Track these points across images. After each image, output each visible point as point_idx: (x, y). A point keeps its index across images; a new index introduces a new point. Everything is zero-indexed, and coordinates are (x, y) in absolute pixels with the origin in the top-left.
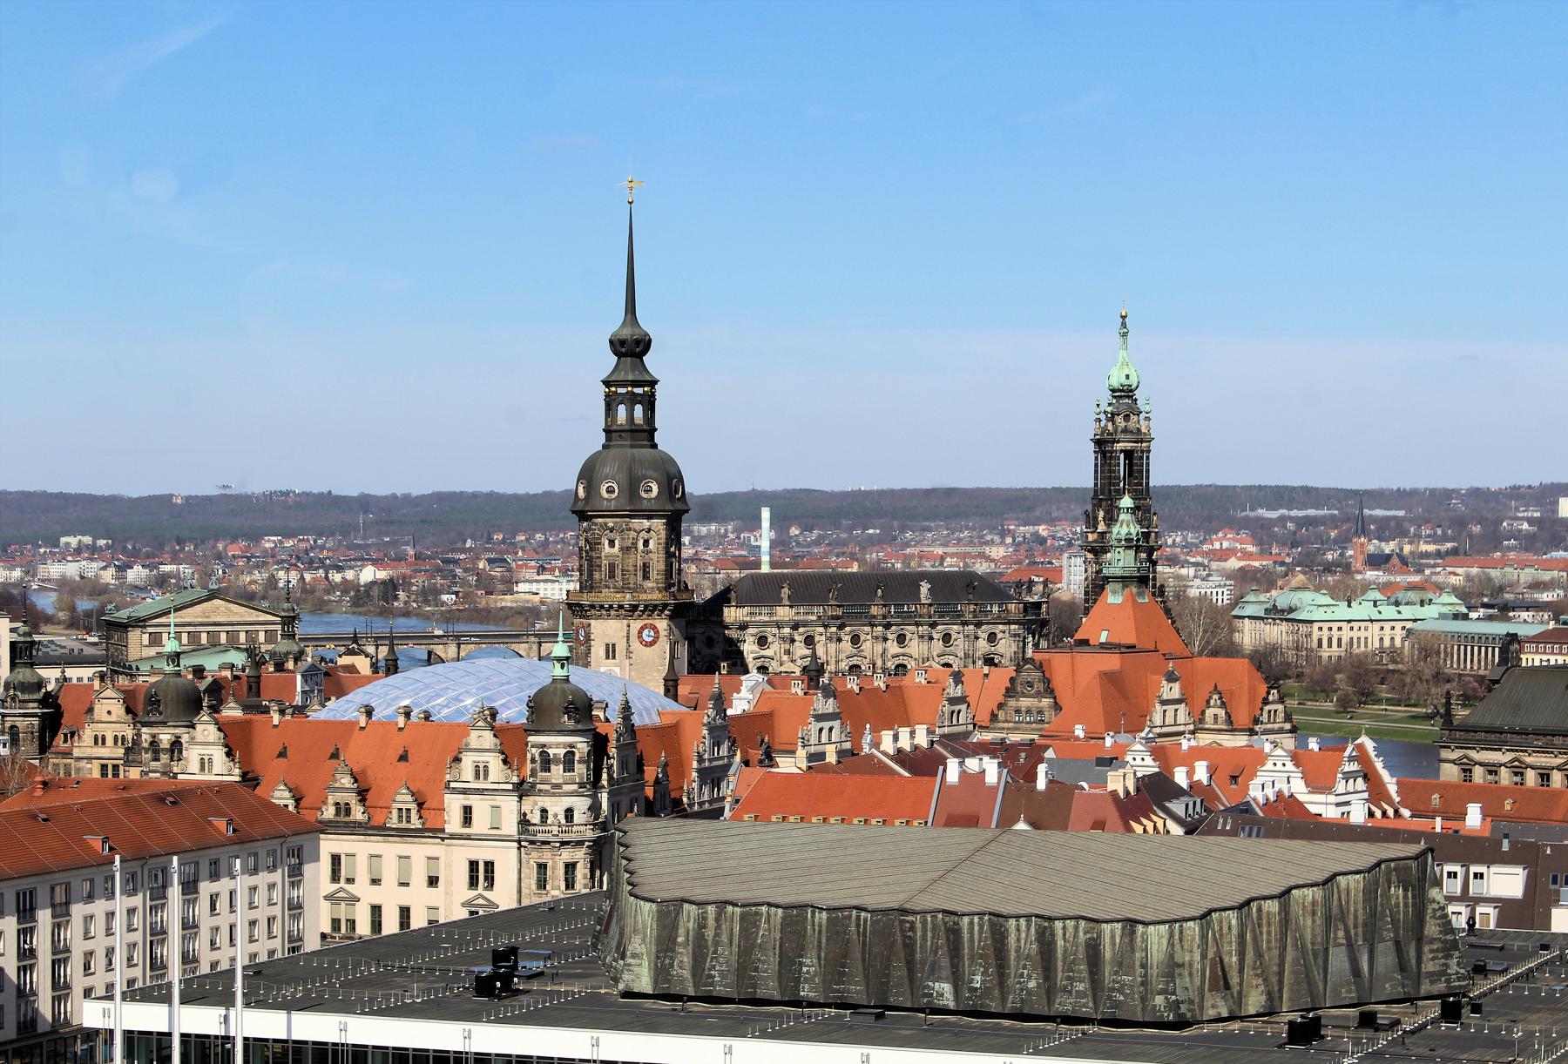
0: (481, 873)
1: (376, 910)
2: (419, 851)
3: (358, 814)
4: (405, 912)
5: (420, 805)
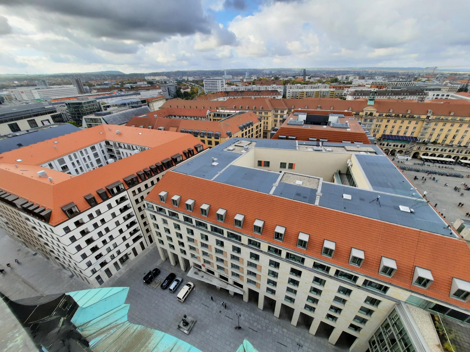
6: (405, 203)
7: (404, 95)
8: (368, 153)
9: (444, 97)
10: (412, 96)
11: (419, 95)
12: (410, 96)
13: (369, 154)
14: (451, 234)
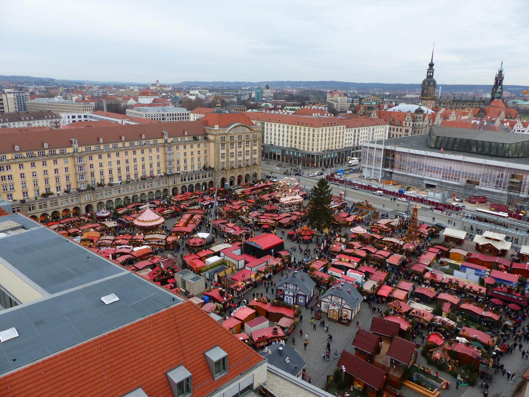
0: (407, 131)
1: (393, 134)
2: (399, 128)
3: (392, 123)
4: (397, 135)
5: (400, 122)
6: (106, 290)
7: (26, 120)
8: (10, 232)
9: (83, 119)
10: (40, 121)
11: (48, 118)
12: (36, 122)
13: (12, 233)
14: (174, 299)
